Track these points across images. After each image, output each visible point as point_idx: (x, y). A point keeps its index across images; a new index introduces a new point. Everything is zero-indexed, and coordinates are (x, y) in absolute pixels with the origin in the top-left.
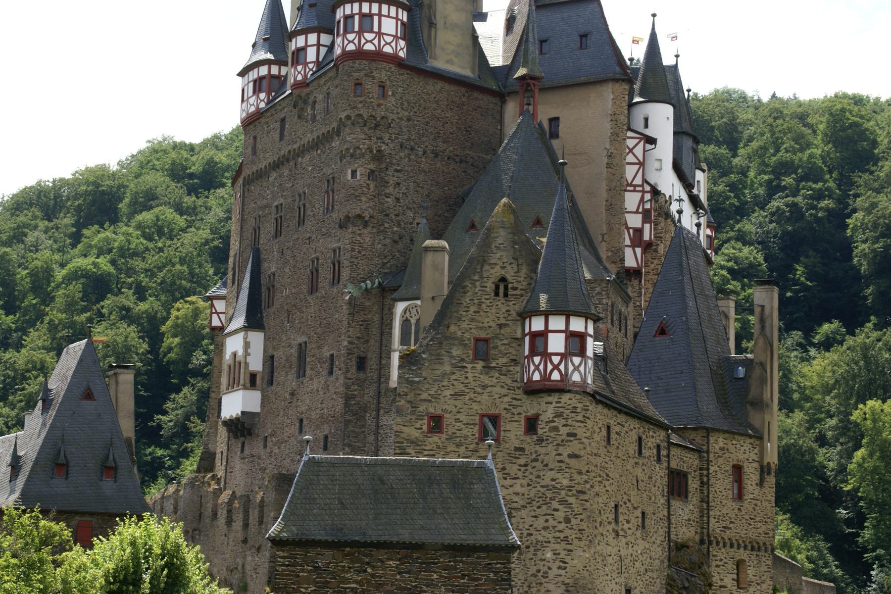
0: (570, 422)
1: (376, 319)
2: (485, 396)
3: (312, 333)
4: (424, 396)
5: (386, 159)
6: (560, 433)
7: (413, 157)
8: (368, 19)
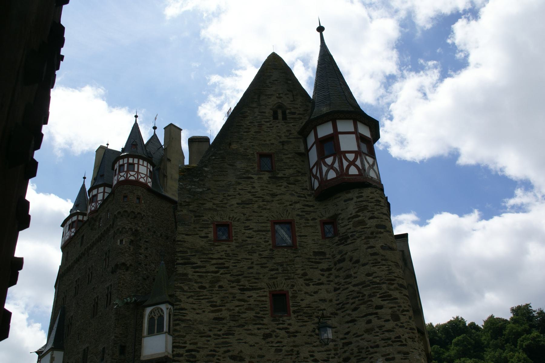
0: (376, 214)
4: (209, 205)
6: (367, 226)
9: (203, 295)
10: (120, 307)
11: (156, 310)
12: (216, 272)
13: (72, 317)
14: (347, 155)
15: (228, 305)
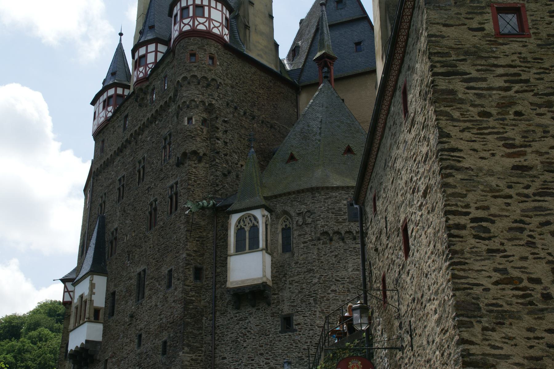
1: (210, 236)
3: (151, 260)
5: (216, 111)
7: (236, 114)
8: (201, 9)
9: (489, 128)
10: (193, 212)
11: (246, 218)
12: (507, 89)
13: (116, 230)
15: (536, 146)
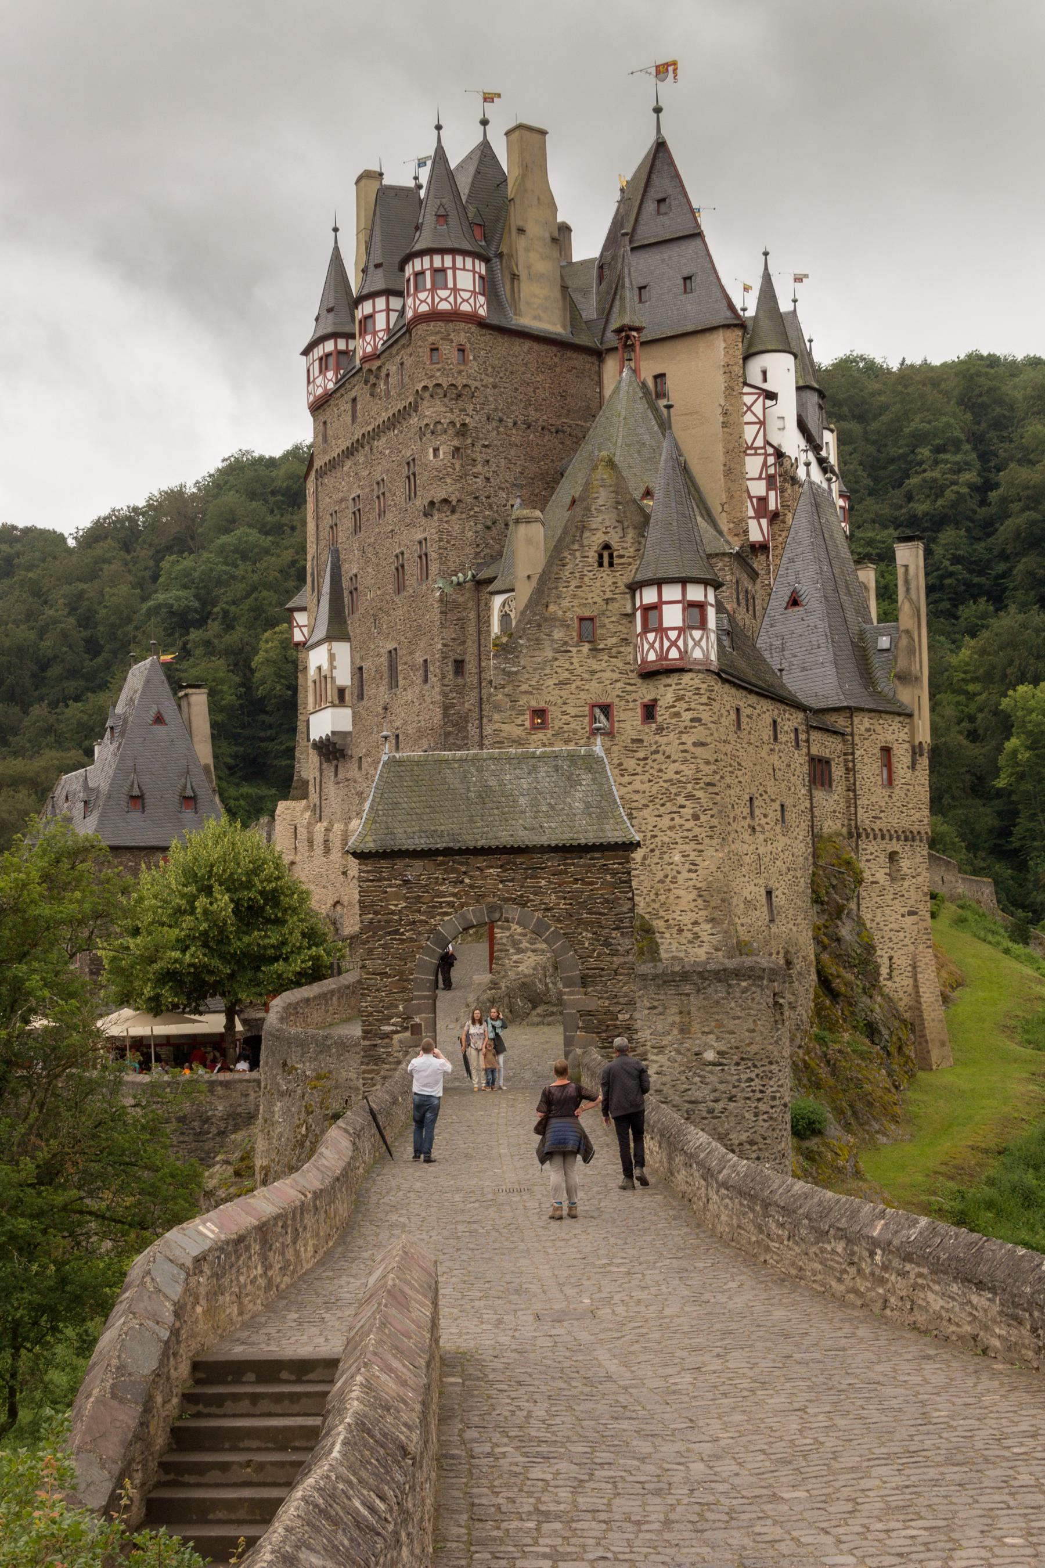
0: (693, 705)
2: (594, 683)
4: (525, 687)
7: (501, 429)
14: (670, 633)
